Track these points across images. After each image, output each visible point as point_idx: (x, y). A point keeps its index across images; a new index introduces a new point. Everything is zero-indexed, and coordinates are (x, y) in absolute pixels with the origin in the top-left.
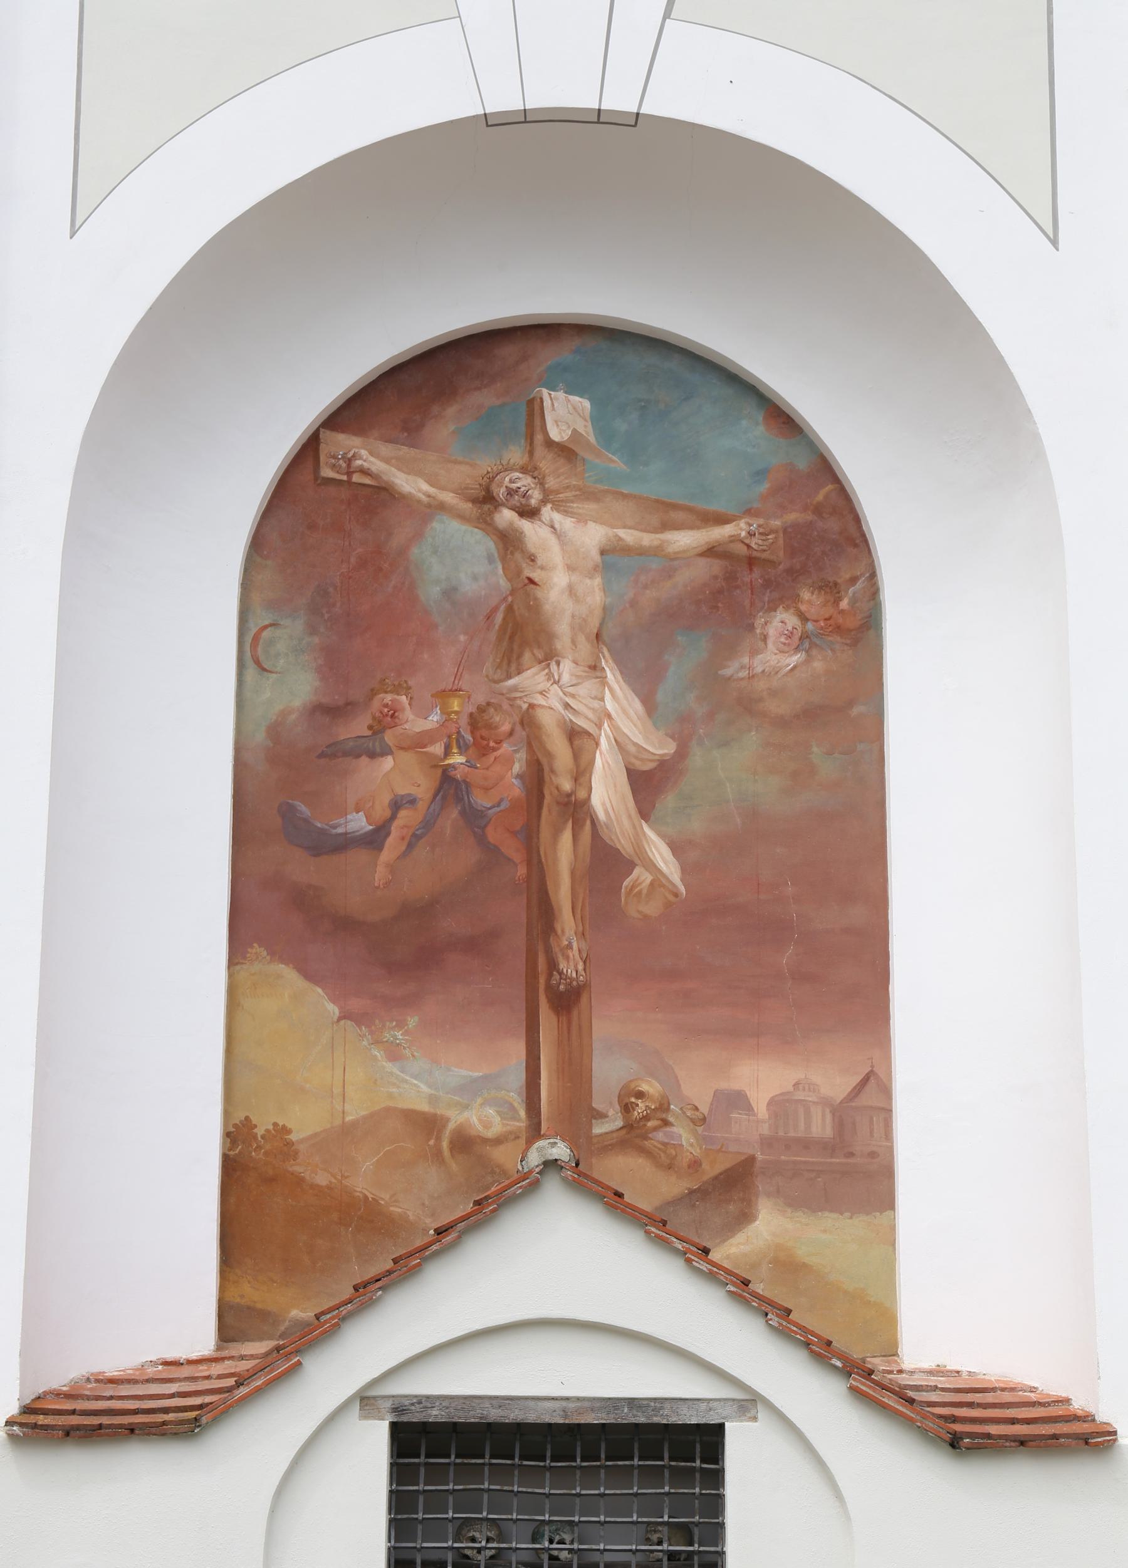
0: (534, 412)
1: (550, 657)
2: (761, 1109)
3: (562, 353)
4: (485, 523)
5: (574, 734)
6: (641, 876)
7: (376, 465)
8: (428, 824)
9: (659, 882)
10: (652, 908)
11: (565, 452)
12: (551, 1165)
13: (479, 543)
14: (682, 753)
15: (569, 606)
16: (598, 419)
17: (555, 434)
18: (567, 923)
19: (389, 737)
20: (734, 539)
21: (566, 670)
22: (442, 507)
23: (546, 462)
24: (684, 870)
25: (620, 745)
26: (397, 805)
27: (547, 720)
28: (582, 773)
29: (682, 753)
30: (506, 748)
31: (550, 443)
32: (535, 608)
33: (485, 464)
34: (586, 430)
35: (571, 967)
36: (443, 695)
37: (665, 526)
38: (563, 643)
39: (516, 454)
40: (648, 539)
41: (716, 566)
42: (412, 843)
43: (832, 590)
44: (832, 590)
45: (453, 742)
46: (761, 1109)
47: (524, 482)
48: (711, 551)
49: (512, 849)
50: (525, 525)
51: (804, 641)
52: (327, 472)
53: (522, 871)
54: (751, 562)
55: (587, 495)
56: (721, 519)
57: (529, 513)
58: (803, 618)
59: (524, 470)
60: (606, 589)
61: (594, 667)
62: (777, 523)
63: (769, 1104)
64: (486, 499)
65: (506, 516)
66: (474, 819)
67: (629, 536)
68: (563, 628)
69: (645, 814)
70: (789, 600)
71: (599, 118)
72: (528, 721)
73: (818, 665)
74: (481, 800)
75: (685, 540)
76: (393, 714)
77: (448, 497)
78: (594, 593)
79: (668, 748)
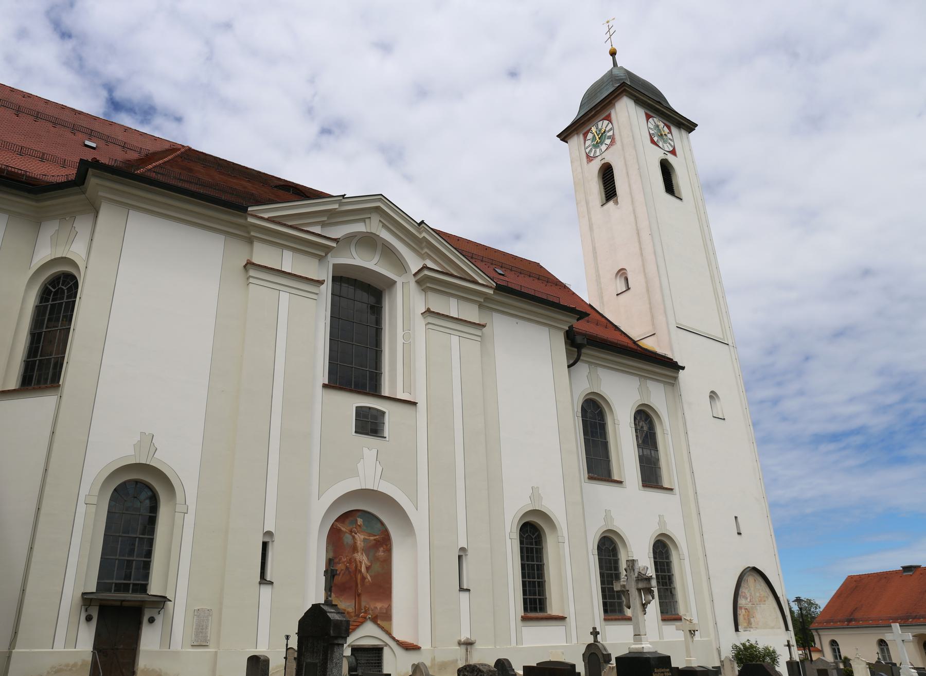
0: (357, 520)
1: (358, 552)
2: (379, 609)
3: (359, 513)
4: (351, 534)
5: (360, 562)
6: (367, 580)
7: (339, 526)
8: (345, 572)
9: (369, 581)
10: (368, 584)
11: (360, 526)
12: (369, 618)
13: (350, 537)
14: (371, 565)
15: (360, 546)
16: (363, 521)
17: (359, 524)
18: (359, 586)
19: (341, 562)
20: (377, 538)
21: (359, 554)
22: (347, 532)
23: (358, 527)
24: (372, 580)
25: (365, 564)
26: (342, 570)
27: (357, 560)
28: (361, 567)
29: (371, 565)
30: (353, 563)
31: (358, 525)
32: (356, 545)
33: (351, 527)
34: (362, 524)
35: (360, 591)
36: (347, 556)
37: (370, 536)
38: (359, 550)
39: (354, 526)
40: (368, 538)
41: (374, 541)
42: (343, 574)
43: (387, 545)
44: (387, 545)
45: (348, 563)
46: (379, 609)
47: (355, 530)
48: (375, 540)
49: (354, 576)
50: (355, 535)
51: (384, 552)
52: (334, 527)
53: (354, 579)
54: (379, 541)
55: (362, 532)
56: (375, 536)
57: (356, 534)
58: (384, 549)
59: (356, 528)
60: (364, 544)
61: (362, 554)
62: (381, 537)
63: (380, 609)
64: (351, 531)
65: (353, 534)
66: (349, 572)
67: (366, 537)
68: (359, 548)
69: (367, 572)
70: (382, 546)
71: (373, 490)
72: (355, 560)
73: (385, 555)
74: (350, 570)
75: (372, 538)
76: (341, 558)
77: (347, 531)
78: (362, 543)
79: (369, 564)
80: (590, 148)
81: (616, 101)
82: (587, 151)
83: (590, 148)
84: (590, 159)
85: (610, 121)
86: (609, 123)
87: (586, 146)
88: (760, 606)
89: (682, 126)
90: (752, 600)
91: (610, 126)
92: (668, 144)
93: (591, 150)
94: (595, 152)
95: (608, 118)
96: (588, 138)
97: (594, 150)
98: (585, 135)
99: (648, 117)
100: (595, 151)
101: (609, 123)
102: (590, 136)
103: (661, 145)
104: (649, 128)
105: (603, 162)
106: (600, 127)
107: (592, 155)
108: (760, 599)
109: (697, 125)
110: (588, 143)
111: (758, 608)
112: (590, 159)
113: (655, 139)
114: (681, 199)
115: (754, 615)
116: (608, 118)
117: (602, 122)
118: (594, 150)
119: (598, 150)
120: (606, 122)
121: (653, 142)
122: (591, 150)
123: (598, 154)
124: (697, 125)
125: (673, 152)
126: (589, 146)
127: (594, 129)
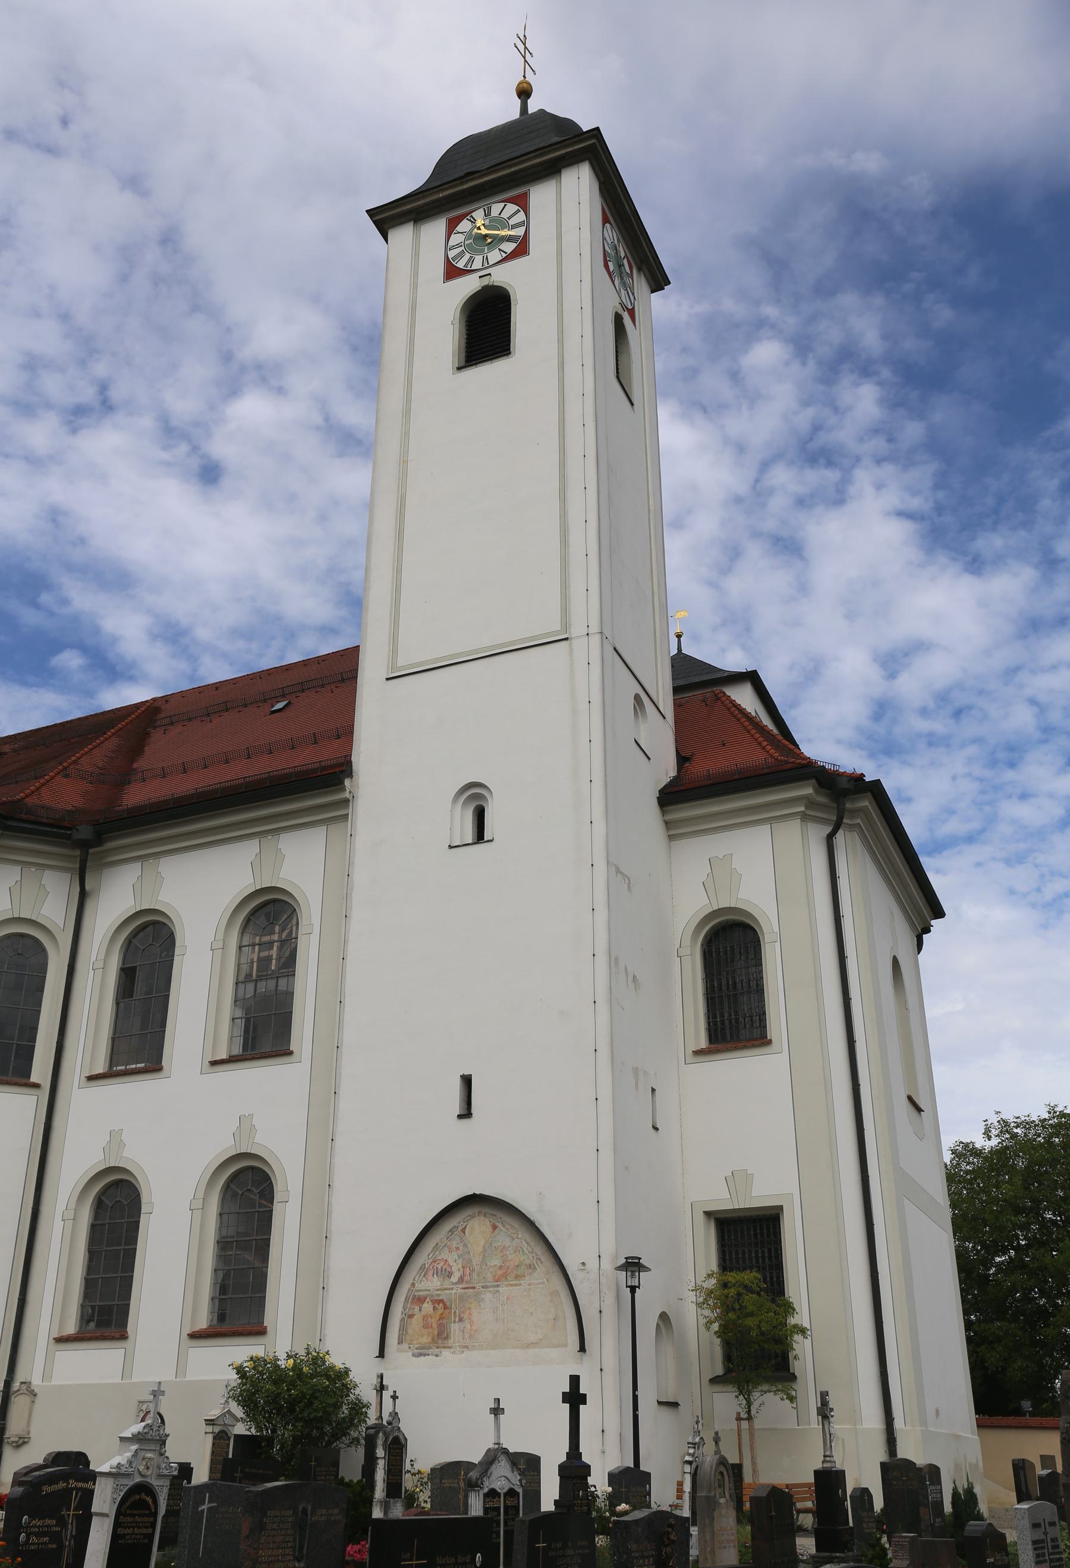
82: (451, 254)
84: (452, 272)
86: (518, 211)
87: (452, 242)
88: (498, 1291)
90: (466, 1278)
93: (461, 255)
94: (471, 260)
96: (459, 228)
97: (467, 256)
101: (518, 211)
102: (464, 226)
105: (486, 281)
107: (461, 264)
108: (500, 1272)
110: (455, 239)
111: (488, 1296)
112: (452, 272)
115: (465, 1316)
116: (523, 202)
117: (503, 204)
118: (467, 256)
120: (512, 208)
122: (461, 255)
123: (477, 264)
126: (458, 245)
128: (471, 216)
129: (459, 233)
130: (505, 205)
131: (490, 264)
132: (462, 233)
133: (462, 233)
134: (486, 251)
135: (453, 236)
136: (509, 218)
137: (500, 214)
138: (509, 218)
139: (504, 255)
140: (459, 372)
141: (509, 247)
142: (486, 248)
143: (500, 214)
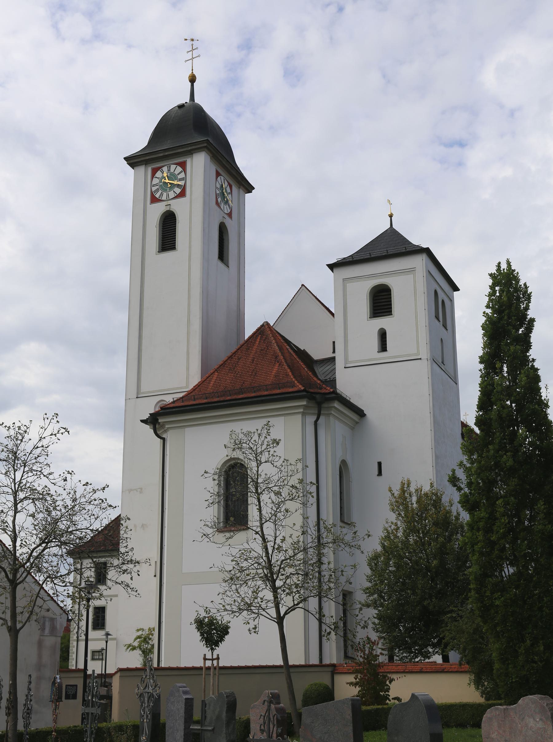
80: (158, 187)
81: (195, 153)
82: (154, 189)
83: (158, 187)
85: (184, 170)
86: (181, 172)
87: (154, 183)
89: (241, 187)
91: (182, 175)
92: (227, 206)
93: (157, 190)
94: (162, 195)
95: (183, 165)
97: (160, 192)
98: (154, 171)
99: (218, 174)
100: (162, 195)
101: (181, 172)
102: (159, 174)
103: (222, 207)
104: (216, 188)
106: (172, 170)
107: (157, 196)
109: (254, 188)
110: (155, 181)
112: (154, 200)
113: (219, 200)
114: (228, 267)
116: (183, 165)
117: (175, 166)
118: (160, 192)
119: (165, 194)
120: (179, 169)
121: (217, 203)
122: (157, 190)
123: (164, 198)
124: (254, 188)
125: (230, 215)
127: (165, 169)
128: (162, 169)
129: (157, 178)
130: (177, 167)
131: (170, 198)
132: (158, 178)
133: (157, 178)
134: (168, 191)
135: (154, 179)
136: (178, 174)
137: (174, 171)
138: (178, 174)
139: (176, 195)
140: (159, 253)
141: (178, 191)
142: (168, 189)
143: (174, 171)
